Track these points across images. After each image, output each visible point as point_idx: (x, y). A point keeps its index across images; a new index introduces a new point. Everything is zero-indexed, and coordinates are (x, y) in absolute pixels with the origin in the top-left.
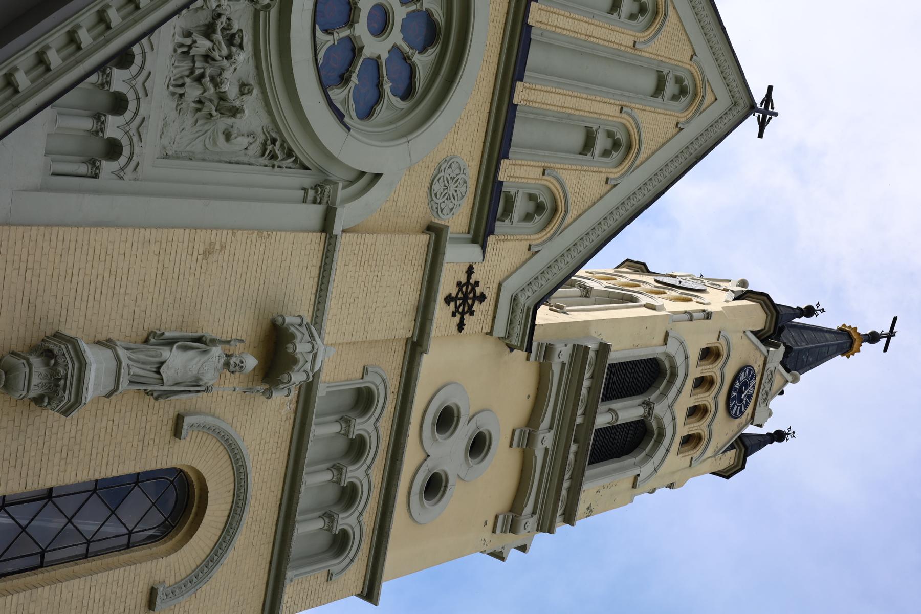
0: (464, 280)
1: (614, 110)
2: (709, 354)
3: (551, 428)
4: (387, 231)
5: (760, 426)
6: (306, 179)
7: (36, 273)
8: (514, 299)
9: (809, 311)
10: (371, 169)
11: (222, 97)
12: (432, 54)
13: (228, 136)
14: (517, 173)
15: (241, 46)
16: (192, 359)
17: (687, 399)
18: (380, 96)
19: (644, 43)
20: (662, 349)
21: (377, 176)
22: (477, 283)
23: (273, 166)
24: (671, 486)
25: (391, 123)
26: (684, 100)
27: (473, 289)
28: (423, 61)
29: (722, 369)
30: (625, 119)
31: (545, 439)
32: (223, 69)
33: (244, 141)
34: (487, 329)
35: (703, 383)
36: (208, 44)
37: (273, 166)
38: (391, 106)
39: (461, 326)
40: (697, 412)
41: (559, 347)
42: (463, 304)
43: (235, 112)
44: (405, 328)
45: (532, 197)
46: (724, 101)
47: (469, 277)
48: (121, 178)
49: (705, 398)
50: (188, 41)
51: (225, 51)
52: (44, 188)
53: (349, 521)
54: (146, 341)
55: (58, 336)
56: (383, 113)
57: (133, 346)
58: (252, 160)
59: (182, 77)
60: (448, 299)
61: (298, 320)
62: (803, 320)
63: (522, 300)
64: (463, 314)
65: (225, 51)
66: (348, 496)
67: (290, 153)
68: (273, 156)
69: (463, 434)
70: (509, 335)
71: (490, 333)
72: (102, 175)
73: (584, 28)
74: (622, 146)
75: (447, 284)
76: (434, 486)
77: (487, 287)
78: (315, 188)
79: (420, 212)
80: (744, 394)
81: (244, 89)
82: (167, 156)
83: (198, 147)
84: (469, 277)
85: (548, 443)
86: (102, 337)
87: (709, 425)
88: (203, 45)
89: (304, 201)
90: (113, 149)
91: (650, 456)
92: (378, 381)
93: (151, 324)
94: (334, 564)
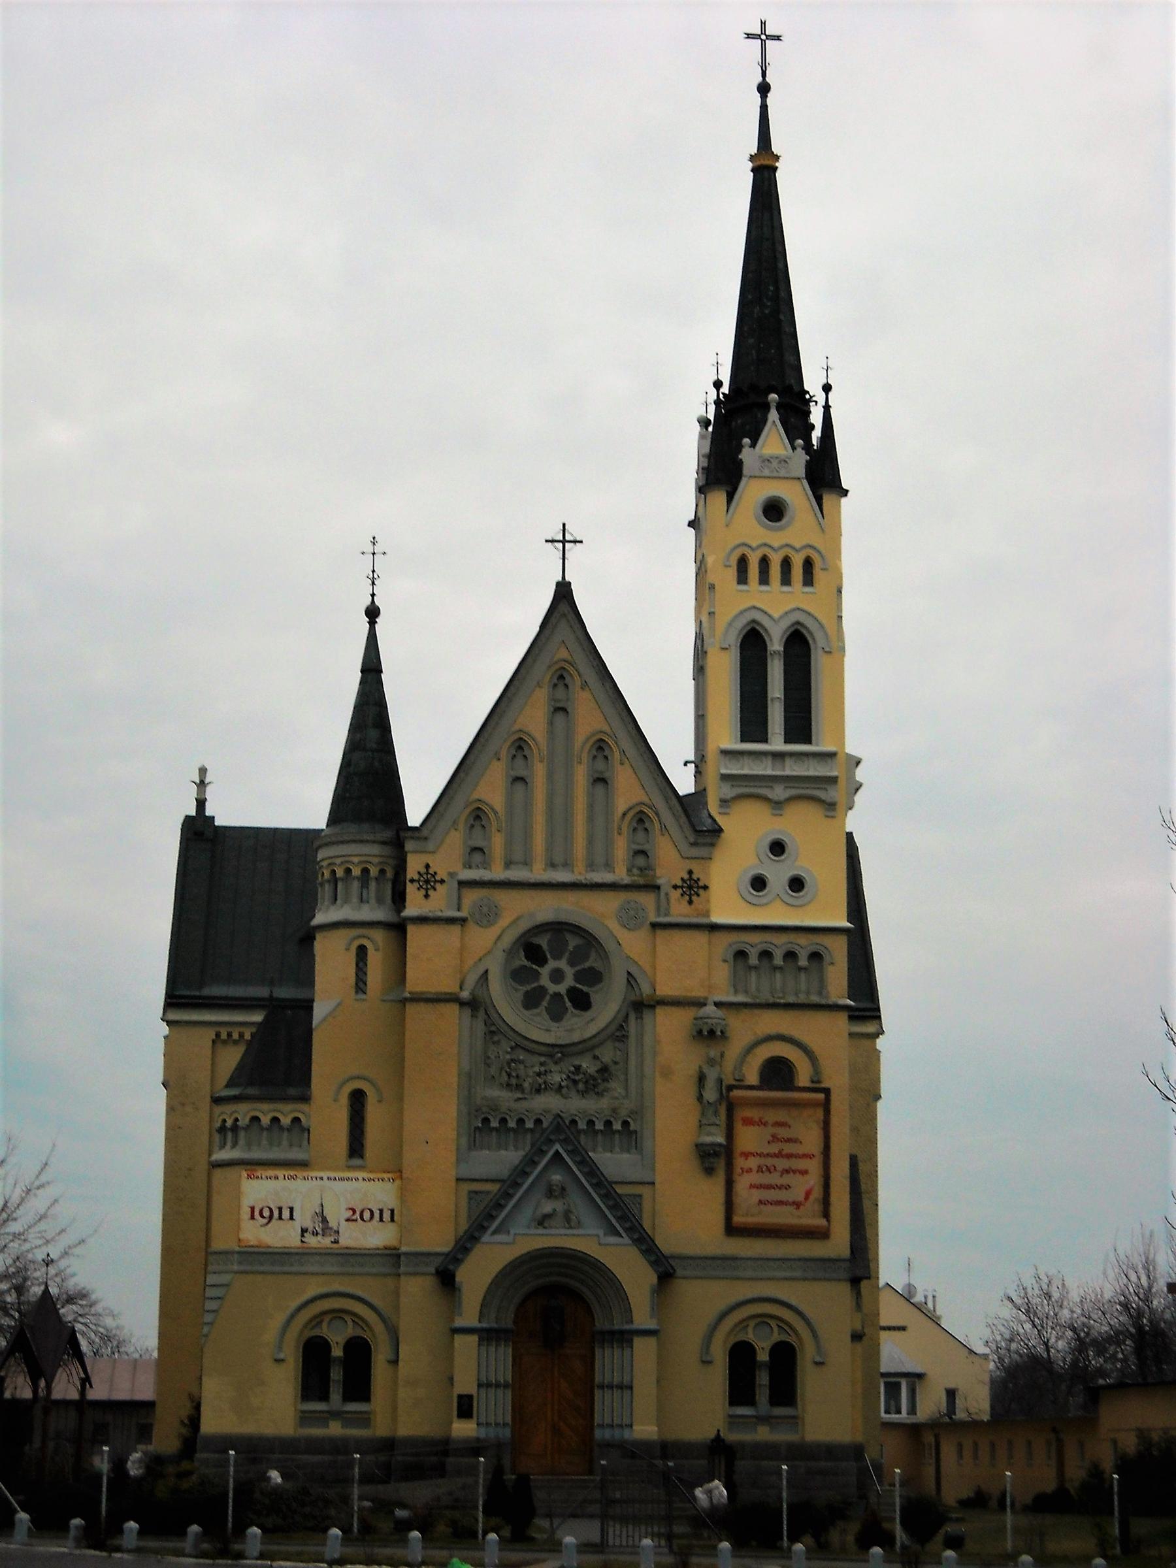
2: (742, 578)
6: (632, 1017)
13: (616, 1063)
18: (591, 969)
22: (682, 879)
26: (568, 680)
44: (702, 938)
63: (692, 840)
65: (581, 1076)
66: (791, 955)
74: (600, 747)
76: (797, 884)
79: (644, 933)
83: (622, 1077)
87: (797, 551)
88: (581, 1086)
90: (626, 1124)
91: (811, 634)
93: (691, 1100)
94: (827, 958)
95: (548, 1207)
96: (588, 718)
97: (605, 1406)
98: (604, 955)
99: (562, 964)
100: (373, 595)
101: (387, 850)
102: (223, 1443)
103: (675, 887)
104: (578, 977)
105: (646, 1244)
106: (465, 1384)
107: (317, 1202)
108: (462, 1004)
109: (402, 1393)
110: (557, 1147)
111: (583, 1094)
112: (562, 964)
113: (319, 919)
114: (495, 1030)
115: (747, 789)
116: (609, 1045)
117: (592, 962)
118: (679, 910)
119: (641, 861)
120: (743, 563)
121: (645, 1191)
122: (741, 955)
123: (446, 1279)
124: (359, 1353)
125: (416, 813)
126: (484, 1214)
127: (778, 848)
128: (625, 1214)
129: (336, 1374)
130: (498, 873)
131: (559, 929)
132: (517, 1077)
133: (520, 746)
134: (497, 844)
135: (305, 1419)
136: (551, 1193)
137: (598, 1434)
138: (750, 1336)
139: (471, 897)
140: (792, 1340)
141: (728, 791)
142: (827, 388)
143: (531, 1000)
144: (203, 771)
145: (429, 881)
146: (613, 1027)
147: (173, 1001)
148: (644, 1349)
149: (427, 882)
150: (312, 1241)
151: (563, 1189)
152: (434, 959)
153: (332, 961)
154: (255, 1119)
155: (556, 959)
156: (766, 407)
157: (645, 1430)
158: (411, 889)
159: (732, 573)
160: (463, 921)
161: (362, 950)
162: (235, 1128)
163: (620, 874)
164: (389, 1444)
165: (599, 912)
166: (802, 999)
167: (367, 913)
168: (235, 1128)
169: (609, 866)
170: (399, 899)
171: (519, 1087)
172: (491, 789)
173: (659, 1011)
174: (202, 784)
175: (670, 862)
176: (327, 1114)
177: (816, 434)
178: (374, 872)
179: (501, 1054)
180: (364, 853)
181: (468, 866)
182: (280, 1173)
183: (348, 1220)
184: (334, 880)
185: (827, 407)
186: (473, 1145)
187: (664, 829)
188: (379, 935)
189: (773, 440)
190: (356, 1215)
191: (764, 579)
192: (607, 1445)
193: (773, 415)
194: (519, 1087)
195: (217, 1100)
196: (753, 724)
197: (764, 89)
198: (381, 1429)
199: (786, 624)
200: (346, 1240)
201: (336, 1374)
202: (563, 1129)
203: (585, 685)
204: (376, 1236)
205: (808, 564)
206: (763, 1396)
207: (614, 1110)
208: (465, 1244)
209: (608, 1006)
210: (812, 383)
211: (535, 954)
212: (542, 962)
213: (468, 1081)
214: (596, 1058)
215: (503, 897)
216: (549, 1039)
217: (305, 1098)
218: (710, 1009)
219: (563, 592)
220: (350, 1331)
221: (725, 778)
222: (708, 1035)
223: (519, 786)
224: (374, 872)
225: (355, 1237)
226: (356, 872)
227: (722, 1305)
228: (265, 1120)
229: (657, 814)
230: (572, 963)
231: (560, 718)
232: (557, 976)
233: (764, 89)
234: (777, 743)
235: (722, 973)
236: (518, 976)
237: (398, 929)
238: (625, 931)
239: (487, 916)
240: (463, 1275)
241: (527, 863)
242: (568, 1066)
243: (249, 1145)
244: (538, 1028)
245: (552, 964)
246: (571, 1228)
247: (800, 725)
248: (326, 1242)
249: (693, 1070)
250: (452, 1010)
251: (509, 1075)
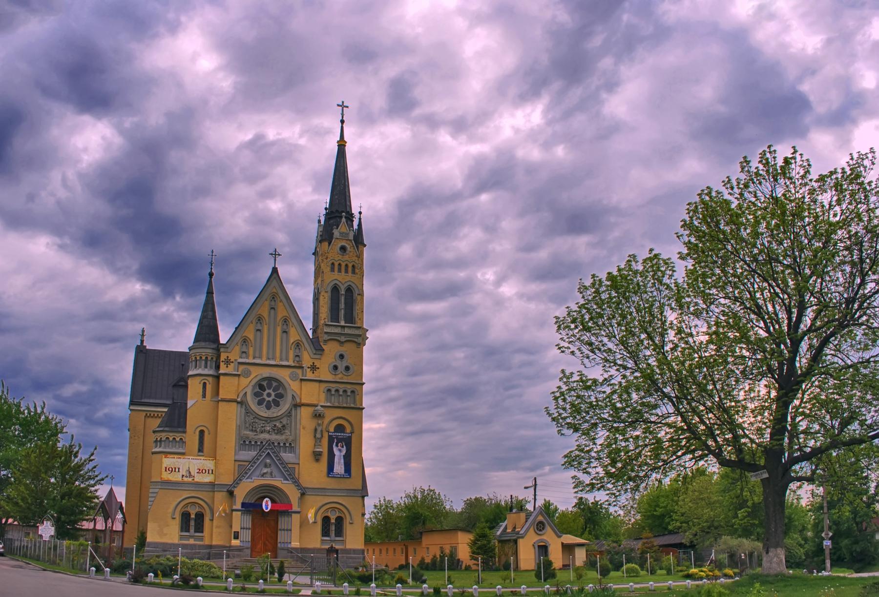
2: (333, 270)
28: (274, 384)
31: (343, 339)
44: (317, 384)
56: (282, 392)
69: (338, 363)
74: (286, 321)
76: (347, 368)
93: (312, 437)
95: (265, 470)
96: (282, 313)
97: (281, 537)
98: (285, 389)
99: (271, 391)
101: (214, 351)
102: (156, 545)
104: (276, 396)
105: (297, 483)
106: (236, 527)
107: (186, 466)
108: (238, 403)
109: (214, 530)
111: (277, 434)
112: (271, 391)
113: (190, 373)
114: (248, 412)
115: (333, 338)
116: (285, 419)
117: (281, 391)
118: (310, 375)
119: (297, 359)
120: (333, 264)
121: (296, 466)
122: (329, 390)
123: (231, 493)
124: (200, 517)
125: (224, 338)
126: (243, 471)
127: (342, 357)
128: (290, 473)
129: (192, 523)
130: (251, 361)
131: (270, 379)
133: (260, 319)
134: (251, 350)
135: (182, 537)
136: (266, 466)
137: (279, 545)
138: (329, 514)
139: (242, 368)
140: (342, 515)
141: (326, 337)
142: (360, 213)
143: (260, 403)
144: (143, 331)
145: (228, 362)
147: (132, 403)
148: (296, 518)
150: (185, 479)
152: (228, 389)
153: (194, 387)
154: (167, 438)
155: (269, 389)
156: (341, 217)
157: (295, 544)
158: (222, 364)
159: (329, 269)
160: (239, 375)
161: (205, 384)
162: (161, 441)
163: (291, 363)
164: (210, 547)
165: (283, 375)
166: (348, 405)
167: (206, 372)
168: (161, 441)
169: (287, 360)
170: (218, 367)
171: (256, 431)
172: (250, 333)
173: (303, 408)
174: (143, 335)
175: (307, 359)
176: (191, 438)
177: (355, 226)
178: (209, 358)
179: (251, 420)
180: (207, 351)
181: (241, 357)
182: (176, 456)
184: (196, 360)
185: (360, 219)
186: (240, 450)
187: (306, 349)
188: (210, 379)
189: (343, 227)
190: (200, 471)
191: (340, 271)
192: (283, 549)
193: (344, 220)
194: (256, 431)
195: (154, 432)
196: (334, 315)
197: (342, 122)
198: (207, 542)
199: (346, 285)
200: (196, 479)
201: (192, 523)
202: (271, 443)
203: (281, 301)
204: (207, 479)
205: (353, 266)
206: (333, 533)
208: (237, 482)
209: (285, 406)
210: (355, 210)
211: (261, 387)
212: (264, 390)
213: (239, 428)
215: (252, 368)
216: (266, 415)
217: (185, 432)
218: (319, 407)
219: (275, 270)
220: (197, 509)
221: (326, 333)
222: (318, 416)
223: (258, 333)
224: (209, 358)
225: (199, 478)
226: (204, 358)
227: (321, 504)
228: (171, 439)
230: (274, 391)
231: (272, 311)
232: (269, 395)
233: (342, 122)
234: (343, 323)
235: (323, 396)
236: (256, 395)
237: (217, 377)
239: (247, 374)
240: (237, 492)
241: (260, 357)
242: (272, 424)
243: (165, 447)
244: (263, 412)
245: (267, 391)
247: (350, 318)
248: (190, 479)
249: (313, 428)
250: (235, 404)
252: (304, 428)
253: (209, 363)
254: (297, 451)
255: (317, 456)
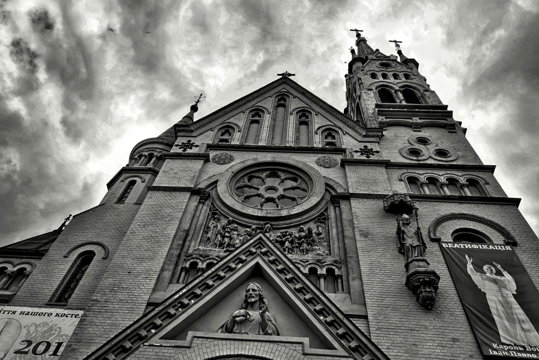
0: (360, 153)
1: (292, 117)
2: (374, 76)
3: (411, 119)
4: (346, 179)
5: (397, 57)
7: (383, 294)
8: (365, 136)
9: (353, 51)
10: (324, 187)
11: (305, 237)
12: (280, 173)
13: (319, 234)
14: (318, 141)
15: (286, 232)
16: (407, 236)
17: (392, 80)
19: (268, 111)
20: (375, 91)
21: (327, 185)
22: (360, 149)
23: (328, 218)
24: (425, 80)
25: (306, 183)
27: (363, 150)
29: (378, 72)
30: (295, 113)
31: (416, 120)
32: (295, 237)
33: (320, 228)
34: (377, 144)
35: (385, 76)
36: (287, 243)
37: (328, 218)
38: (300, 184)
39: (377, 152)
40: (396, 76)
41: (380, 120)
42: (369, 152)
43: (310, 231)
45: (326, 137)
46: (284, 86)
47: (359, 152)
48: (341, 267)
49: (390, 74)
50: (287, 249)
51: (289, 237)
52: (349, 293)
53: (462, 180)
54: (403, 254)
55: (407, 284)
57: (406, 258)
58: (327, 225)
59: (300, 250)
60: (368, 157)
61: (385, 202)
62: (356, 52)
63: (364, 133)
64: (373, 152)
66: (452, 182)
67: (322, 214)
68: (324, 219)
70: (378, 136)
71: (379, 143)
72: (340, 274)
73: (265, 129)
75: (364, 158)
77: (362, 146)
78: (333, 204)
80: (386, 62)
81: (301, 230)
82: (330, 253)
84: (359, 152)
85: (417, 118)
86: (405, 270)
88: (287, 244)
89: (339, 207)
90: (330, 271)
91: (415, 88)
92: (403, 176)
94: (482, 183)
100: (196, 104)
103: (356, 152)
108: (194, 192)
110: (258, 260)
132: (231, 238)
146: (315, 213)
149: (187, 146)
151: (261, 299)
161: (133, 183)
183: (17, 352)
207: (319, 261)
214: (301, 230)
229: (340, 128)
238: (323, 168)
246: (266, 333)
251: (223, 237)
252: (365, 235)
253: (154, 159)
254: (355, 284)
255: (421, 291)
